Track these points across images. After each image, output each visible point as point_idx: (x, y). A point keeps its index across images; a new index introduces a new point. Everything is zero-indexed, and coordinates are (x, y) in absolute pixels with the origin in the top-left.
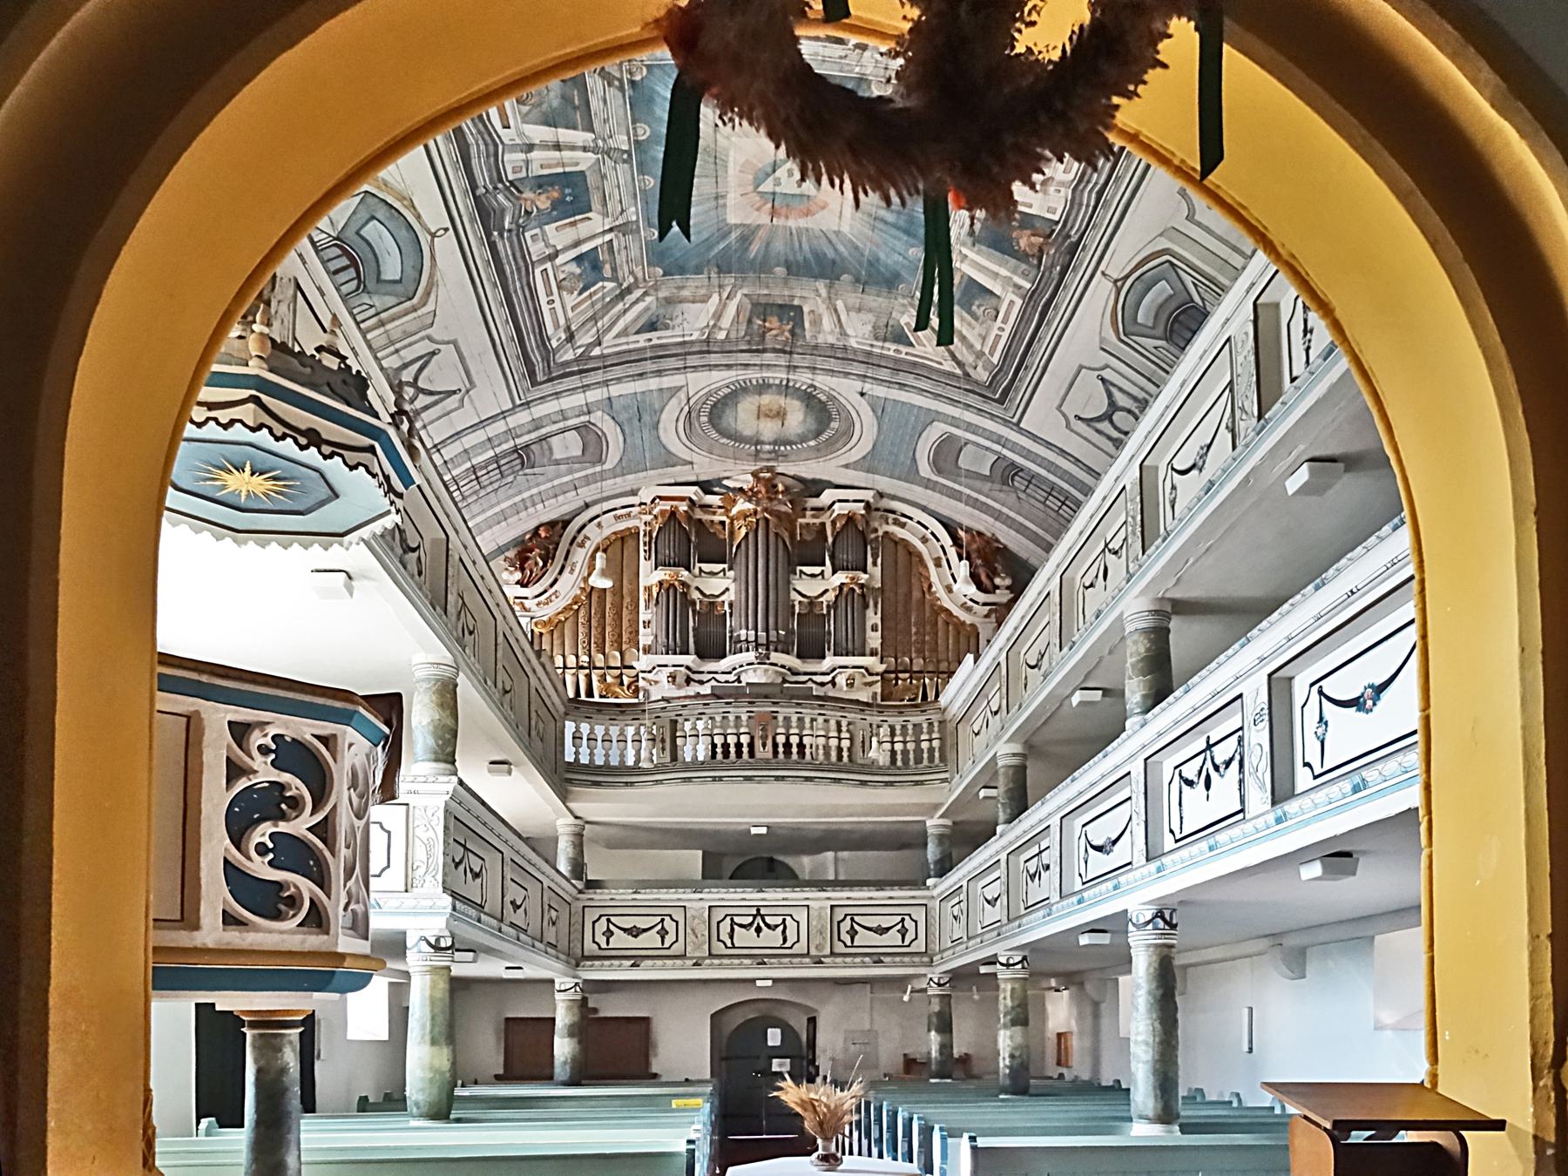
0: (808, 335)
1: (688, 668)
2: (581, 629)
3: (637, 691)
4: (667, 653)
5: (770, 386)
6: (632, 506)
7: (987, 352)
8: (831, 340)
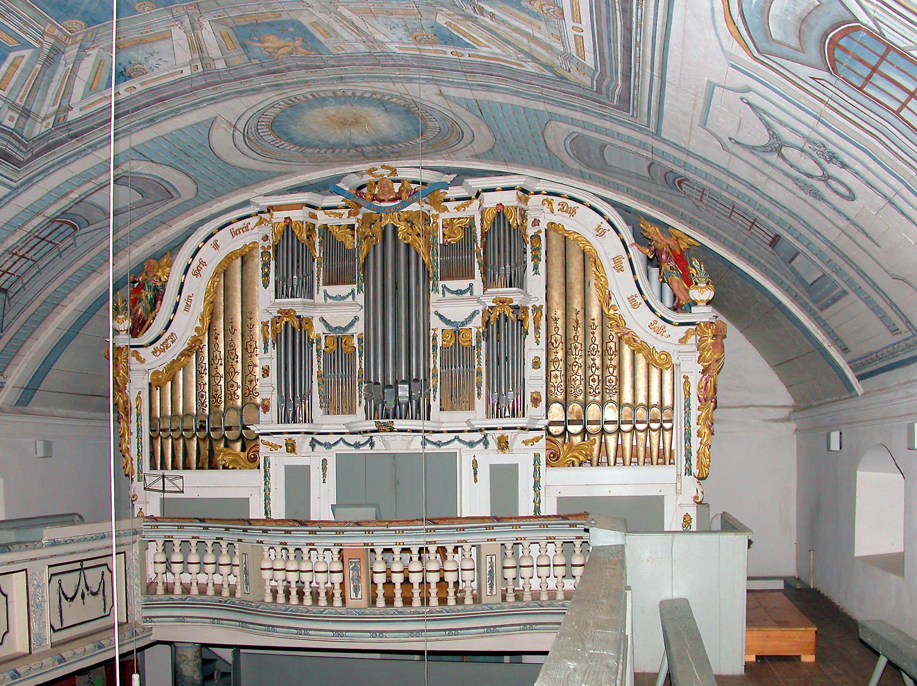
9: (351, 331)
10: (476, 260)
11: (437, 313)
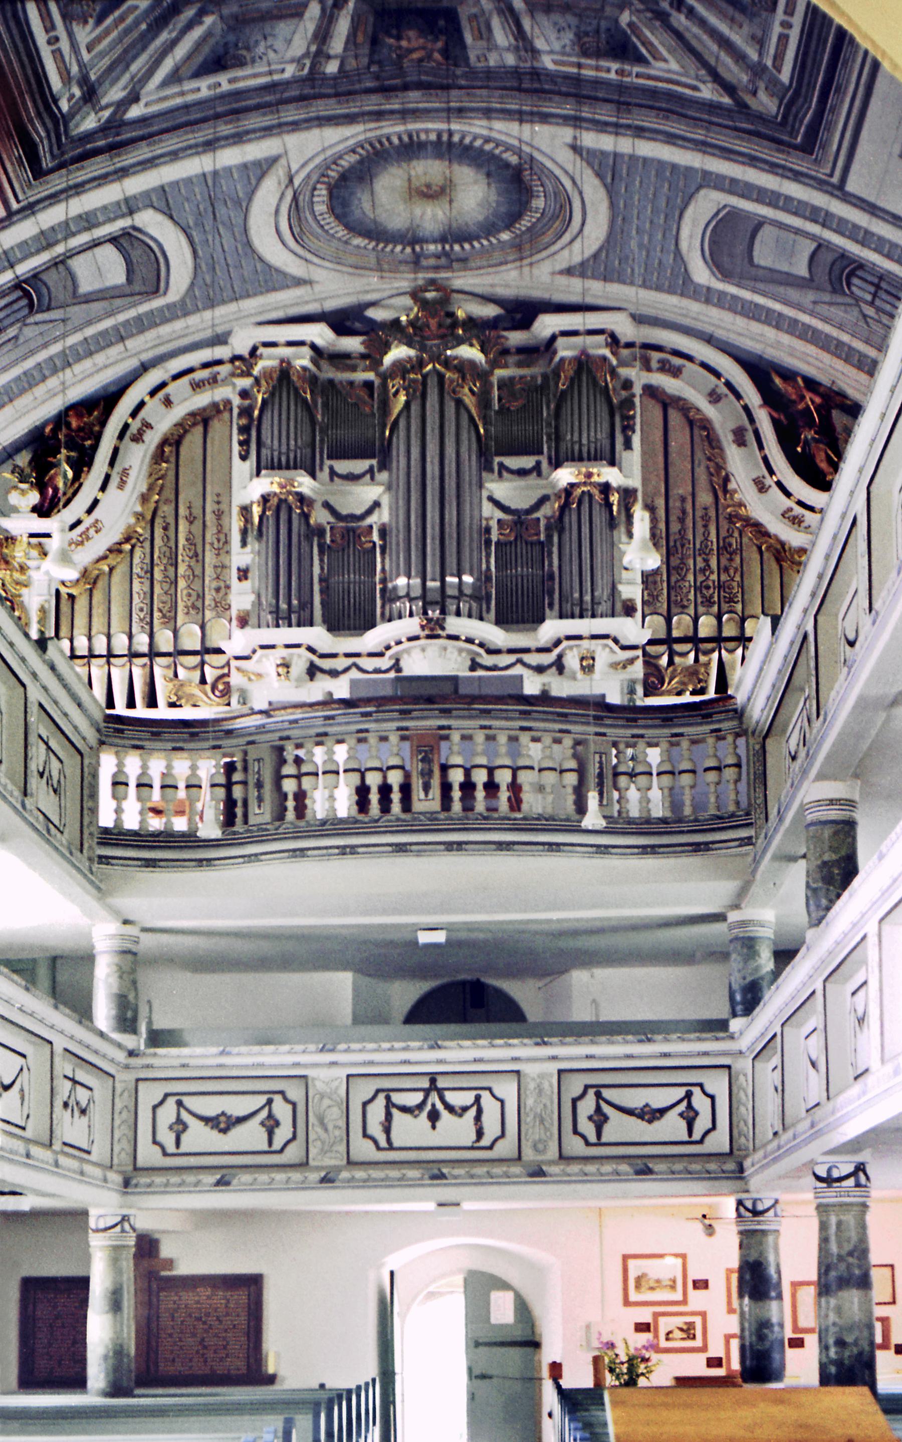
1: (310, 649)
2: (136, 586)
3: (227, 692)
4: (278, 626)
5: (422, 146)
7: (769, 63)
8: (510, 60)
9: (369, 520)
11: (491, 499)
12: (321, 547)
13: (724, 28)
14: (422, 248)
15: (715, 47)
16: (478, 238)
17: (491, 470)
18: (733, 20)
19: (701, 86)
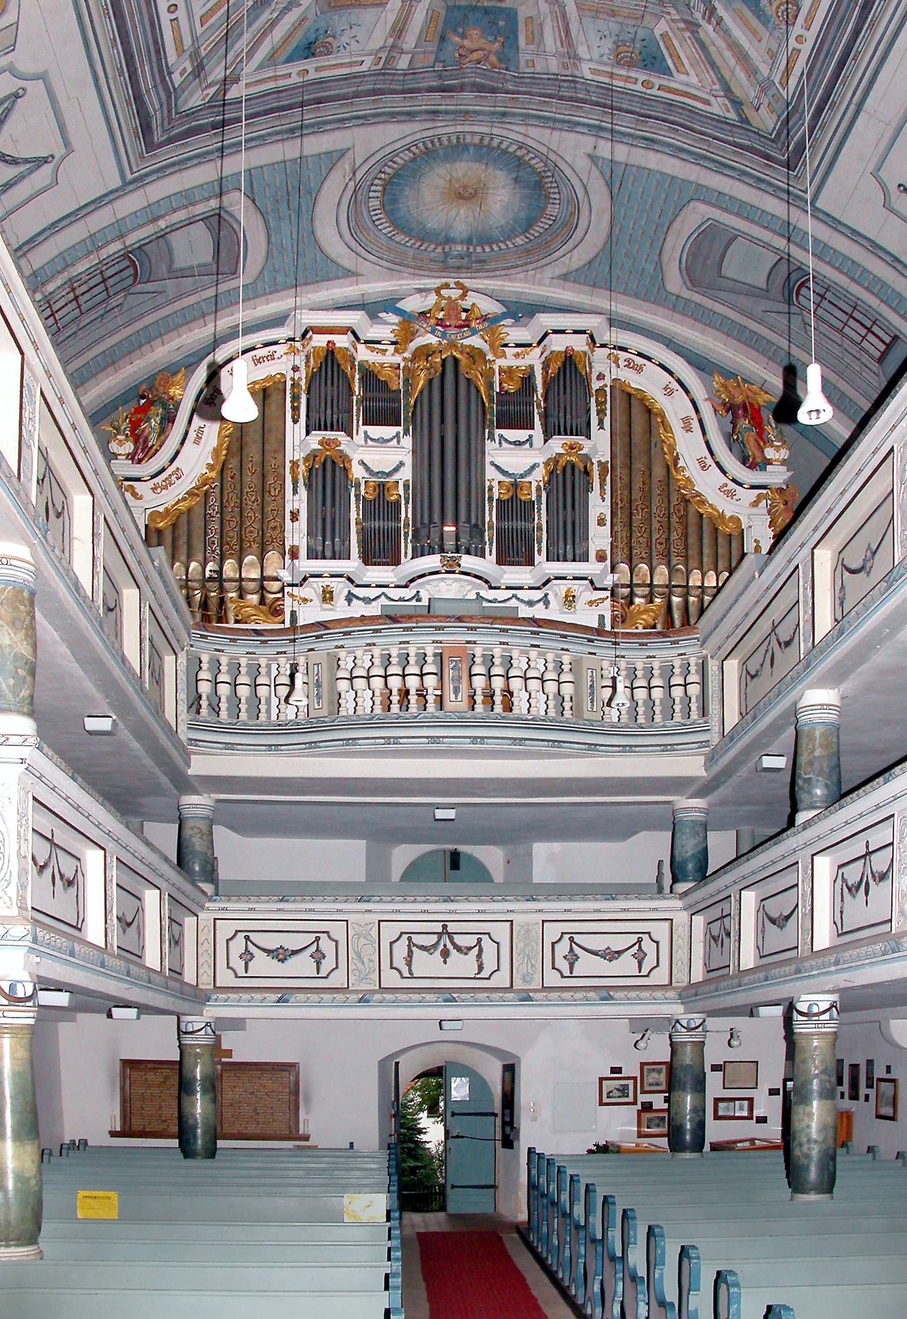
0: (523, 57)
6: (275, 343)
9: (395, 477)
10: (536, 411)
11: (492, 464)
12: (357, 496)
13: (745, 42)
14: (451, 249)
15: (732, 62)
16: (497, 242)
17: (493, 439)
18: (755, 33)
19: (712, 99)
